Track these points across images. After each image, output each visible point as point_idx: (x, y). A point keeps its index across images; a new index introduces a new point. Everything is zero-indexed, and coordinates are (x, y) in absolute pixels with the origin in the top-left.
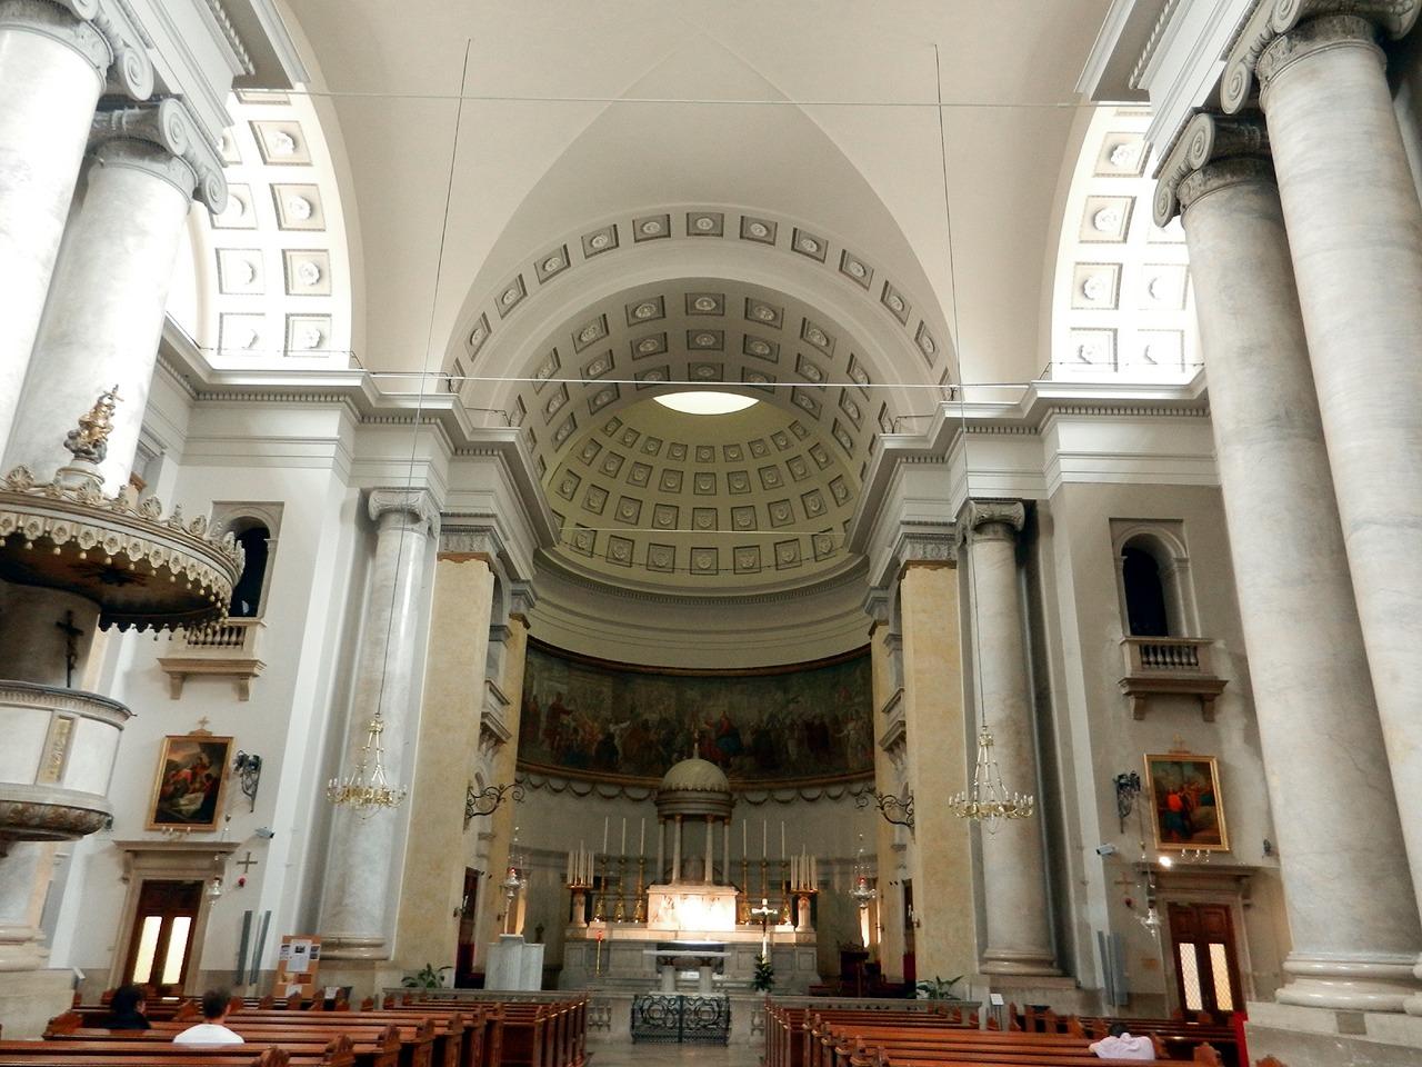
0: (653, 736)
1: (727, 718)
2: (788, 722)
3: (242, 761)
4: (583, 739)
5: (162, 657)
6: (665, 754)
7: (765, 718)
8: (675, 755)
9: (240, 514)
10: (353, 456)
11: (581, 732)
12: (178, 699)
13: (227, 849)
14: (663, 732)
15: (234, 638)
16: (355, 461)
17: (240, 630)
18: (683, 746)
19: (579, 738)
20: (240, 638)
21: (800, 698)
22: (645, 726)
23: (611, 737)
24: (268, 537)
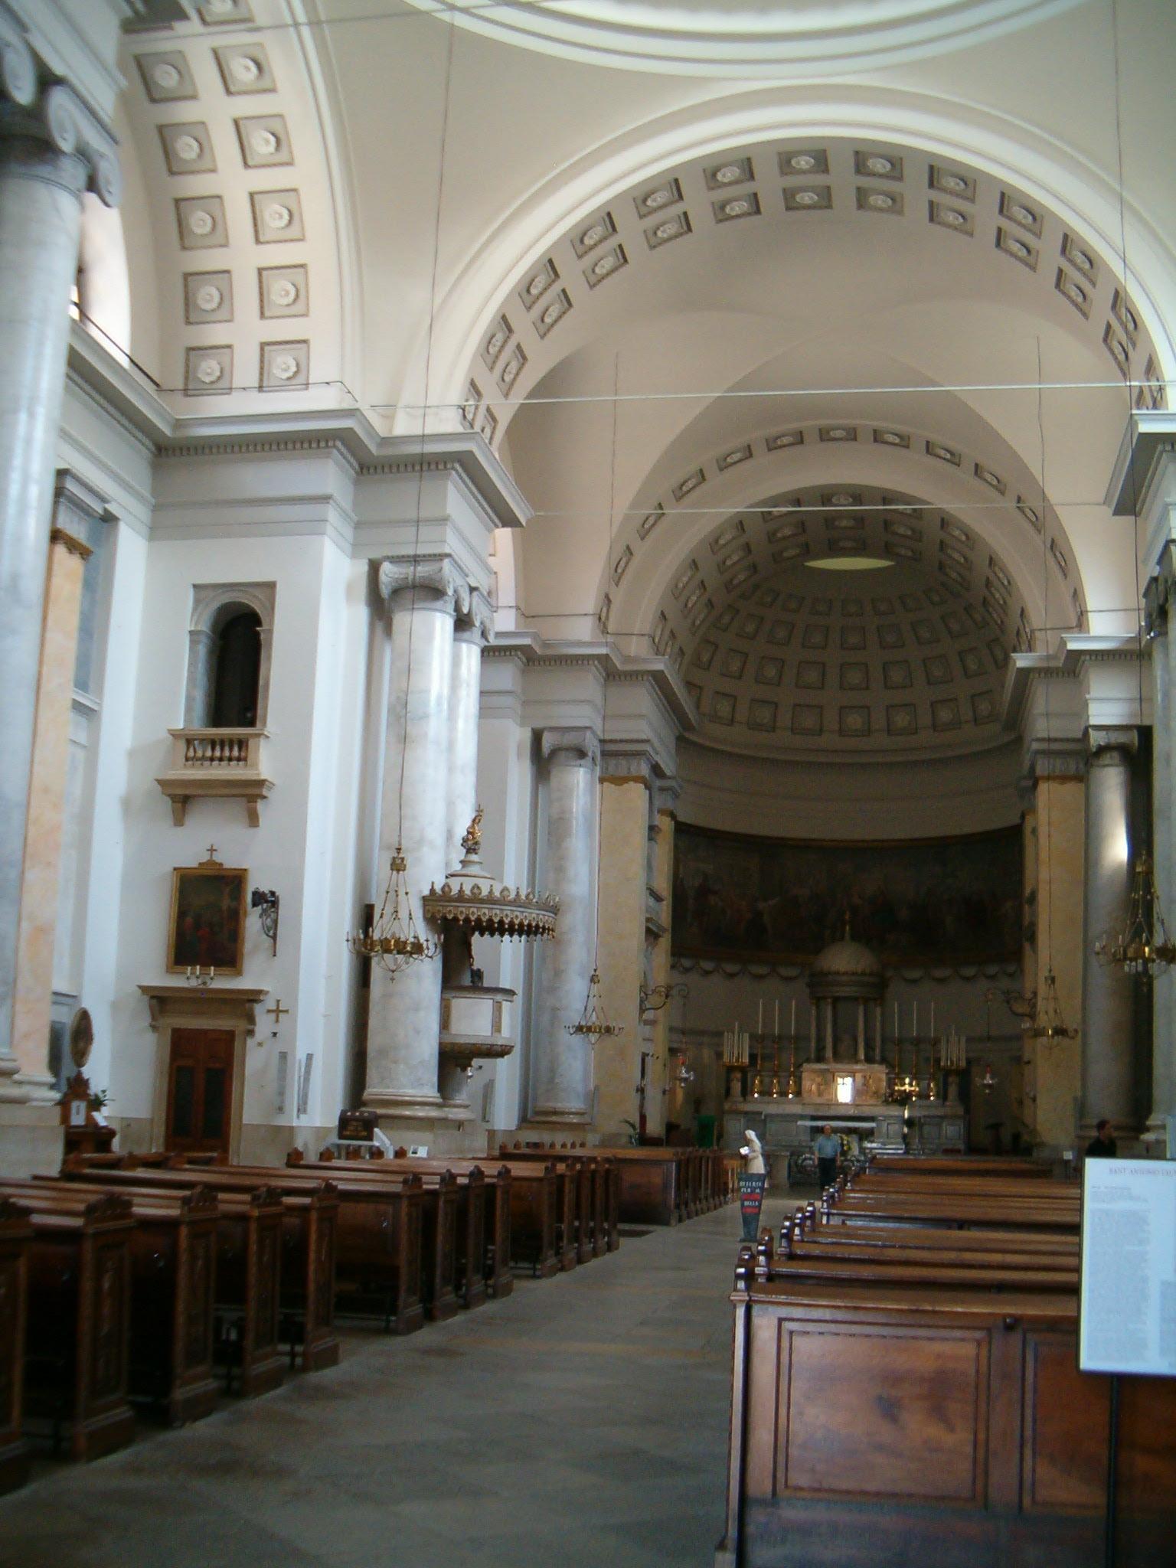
3: (259, 898)
5: (159, 778)
9: (226, 598)
10: (355, 518)
13: (254, 997)
15: (236, 753)
16: (358, 526)
17: (242, 744)
20: (243, 754)
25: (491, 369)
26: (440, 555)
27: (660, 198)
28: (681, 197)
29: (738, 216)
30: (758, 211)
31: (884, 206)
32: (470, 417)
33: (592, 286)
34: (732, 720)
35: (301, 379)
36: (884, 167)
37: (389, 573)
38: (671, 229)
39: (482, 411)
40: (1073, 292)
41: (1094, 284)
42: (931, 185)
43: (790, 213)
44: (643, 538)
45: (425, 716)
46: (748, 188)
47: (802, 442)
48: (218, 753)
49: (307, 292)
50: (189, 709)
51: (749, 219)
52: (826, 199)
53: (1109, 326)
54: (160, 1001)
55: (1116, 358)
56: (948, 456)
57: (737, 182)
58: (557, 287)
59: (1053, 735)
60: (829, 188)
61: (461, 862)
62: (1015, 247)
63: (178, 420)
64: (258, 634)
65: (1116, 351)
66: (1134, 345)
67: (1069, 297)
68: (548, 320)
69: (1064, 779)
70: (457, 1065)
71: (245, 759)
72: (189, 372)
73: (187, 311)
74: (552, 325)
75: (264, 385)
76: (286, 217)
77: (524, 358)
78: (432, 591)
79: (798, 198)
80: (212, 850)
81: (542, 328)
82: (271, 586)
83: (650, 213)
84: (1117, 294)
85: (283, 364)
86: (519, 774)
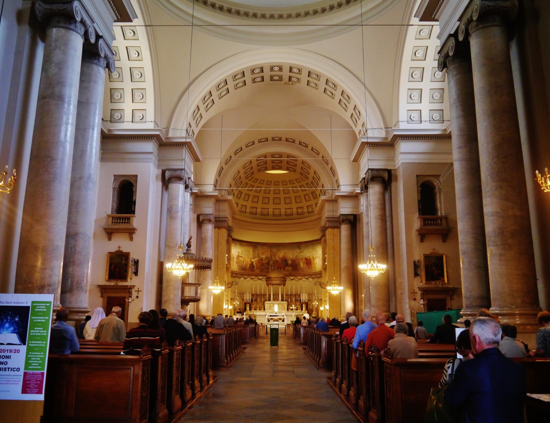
0: (264, 262)
1: (284, 257)
2: (301, 258)
4: (245, 264)
6: (267, 267)
7: (294, 256)
8: (270, 267)
11: (245, 262)
12: (111, 240)
14: (267, 261)
15: (127, 221)
16: (159, 161)
17: (129, 219)
18: (272, 265)
19: (244, 263)
20: (129, 221)
21: (304, 252)
22: (262, 259)
23: (252, 263)
24: (133, 187)
25: (194, 119)
26: (182, 169)
27: (239, 76)
28: (244, 76)
29: (258, 82)
30: (263, 81)
31: (296, 81)
32: (189, 132)
33: (220, 99)
34: (256, 214)
35: (144, 120)
36: (297, 71)
37: (167, 174)
38: (241, 84)
39: (191, 131)
40: (343, 105)
41: (349, 103)
42: (309, 76)
43: (272, 82)
44: (226, 165)
45: (178, 211)
46: (261, 74)
47: (267, 141)
48: (119, 221)
49: (146, 96)
50: (112, 209)
51: (261, 83)
52: (281, 78)
53: (352, 114)
54: (103, 289)
55: (354, 122)
56: (305, 145)
57: (259, 73)
58: (211, 99)
59: (334, 216)
60: (282, 76)
61: (186, 250)
62: (329, 93)
63: (109, 129)
64: (133, 189)
65: (354, 120)
66: (359, 119)
67: (342, 106)
68: (208, 107)
69: (334, 227)
70: (186, 304)
71: (129, 223)
72: (112, 116)
73: (111, 99)
74: (209, 108)
75: (134, 121)
76: (140, 75)
77: (202, 117)
78: (180, 178)
79: (274, 78)
80: (119, 247)
81: (207, 109)
82: (136, 176)
83: (236, 80)
84: (355, 106)
85: (138, 115)
86: (195, 225)
